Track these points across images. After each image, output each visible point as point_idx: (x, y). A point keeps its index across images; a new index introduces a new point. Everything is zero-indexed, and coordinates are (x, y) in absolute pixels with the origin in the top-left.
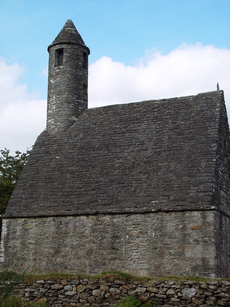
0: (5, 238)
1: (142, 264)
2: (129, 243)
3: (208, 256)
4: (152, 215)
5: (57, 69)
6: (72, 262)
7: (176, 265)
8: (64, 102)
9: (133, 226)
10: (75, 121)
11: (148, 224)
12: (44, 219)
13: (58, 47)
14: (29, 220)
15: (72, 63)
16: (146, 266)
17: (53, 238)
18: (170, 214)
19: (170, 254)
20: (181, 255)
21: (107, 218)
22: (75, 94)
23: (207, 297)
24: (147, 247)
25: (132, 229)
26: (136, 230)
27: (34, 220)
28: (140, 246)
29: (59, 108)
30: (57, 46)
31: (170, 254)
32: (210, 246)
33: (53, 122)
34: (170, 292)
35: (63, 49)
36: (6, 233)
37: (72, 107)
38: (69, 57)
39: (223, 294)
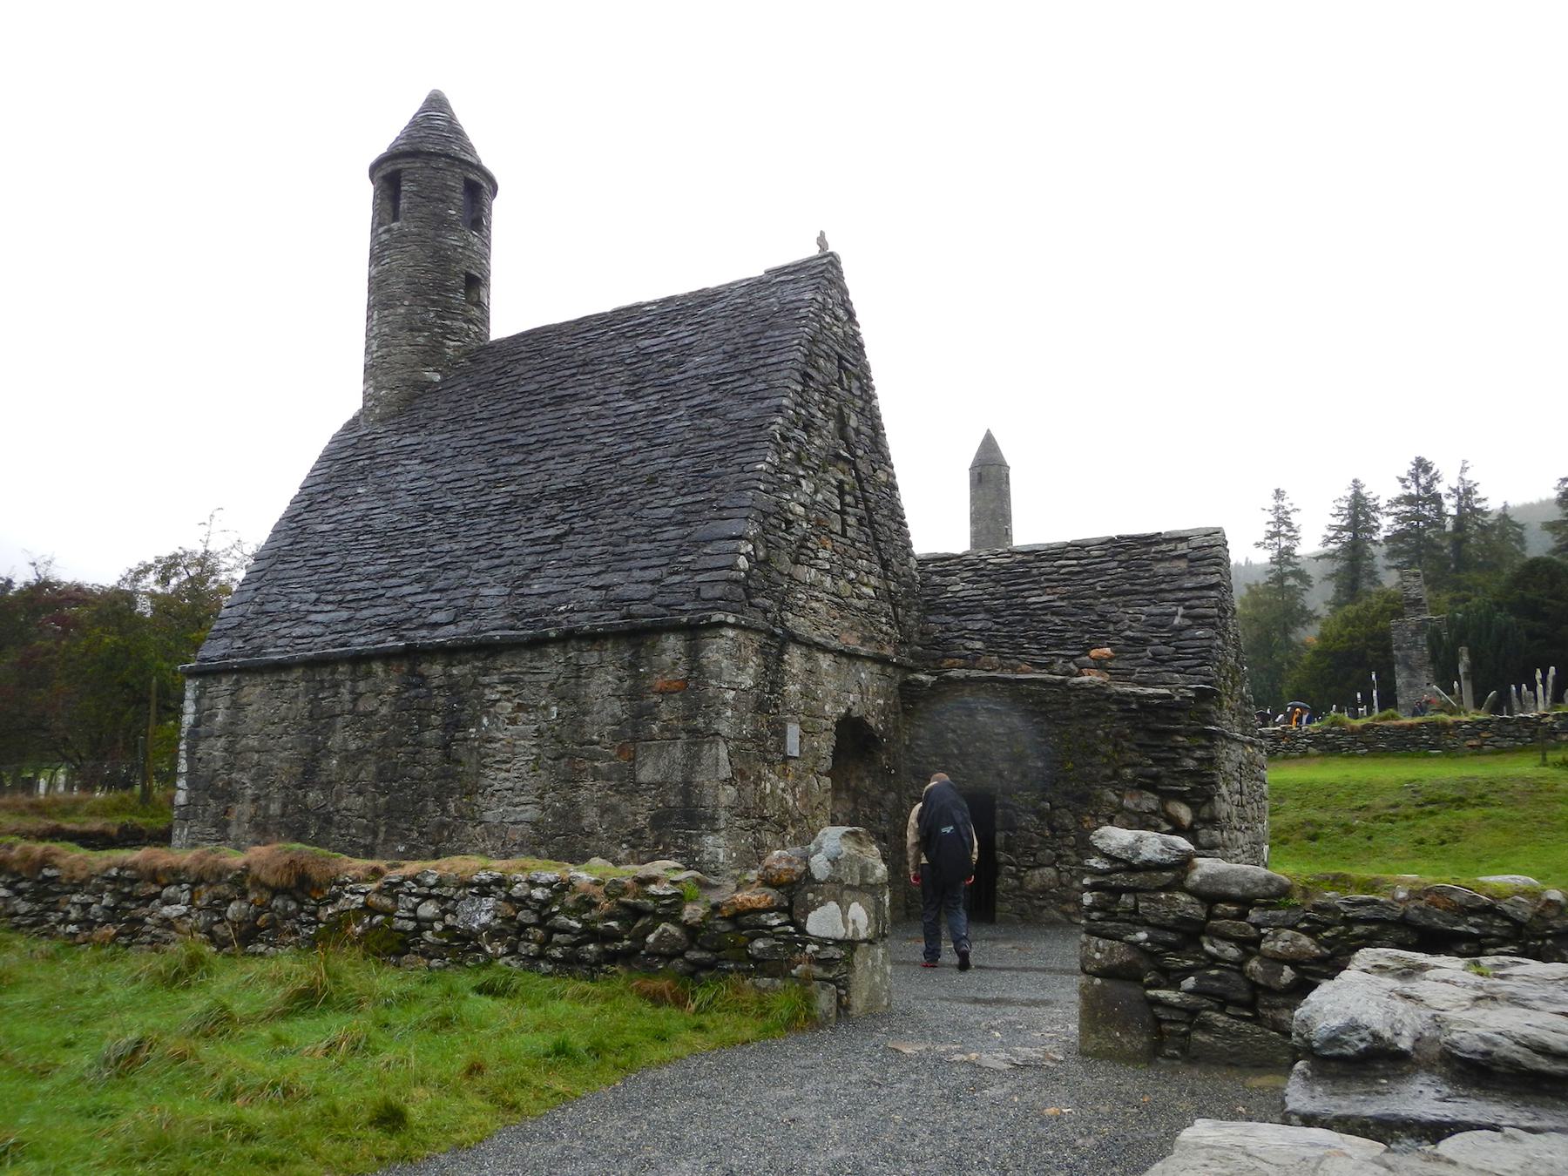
1: (522, 808)
2: (491, 742)
3: (699, 779)
4: (552, 650)
5: (384, 232)
6: (343, 804)
7: (613, 809)
8: (401, 329)
9: (500, 688)
10: (432, 382)
11: (541, 677)
12: (284, 677)
13: (388, 168)
14: (245, 682)
15: (424, 210)
16: (531, 813)
17: (301, 732)
18: (601, 646)
19: (596, 773)
21: (435, 670)
22: (434, 302)
23: (523, 927)
24: (535, 750)
25: (498, 696)
26: (509, 700)
28: (517, 750)
29: (387, 346)
30: (384, 166)
31: (596, 773)
32: (707, 746)
35: (400, 171)
37: (421, 340)
38: (416, 194)
39: (562, 919)
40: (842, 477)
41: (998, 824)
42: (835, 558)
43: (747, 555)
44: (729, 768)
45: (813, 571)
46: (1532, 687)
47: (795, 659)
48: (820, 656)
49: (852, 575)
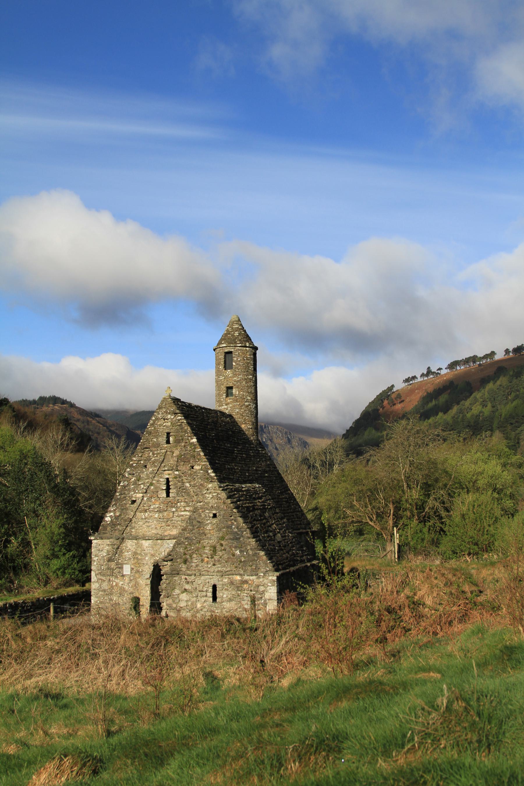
40: (167, 476)
42: (161, 507)
43: (111, 517)
44: (96, 578)
45: (147, 514)
47: (130, 544)
48: (144, 542)
49: (174, 509)
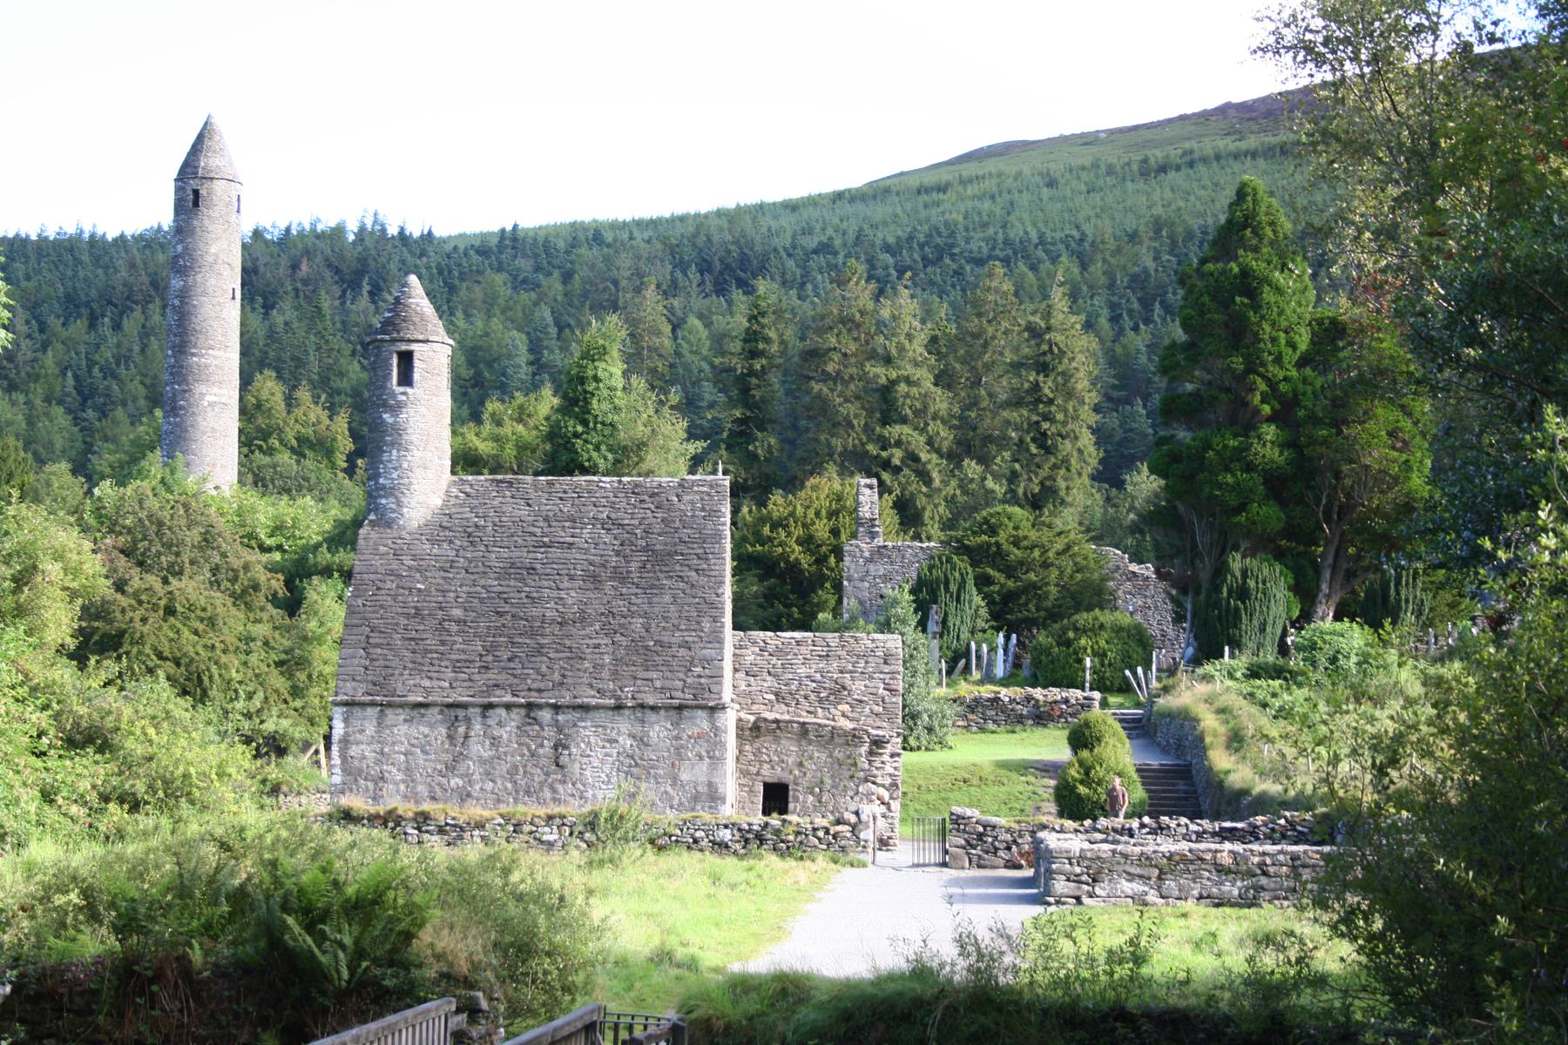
0: (340, 741)
4: (627, 712)
12: (422, 711)
14: (389, 711)
20: (675, 780)
27: (401, 711)
33: (393, 506)
34: (699, 834)
36: (342, 732)
41: (791, 799)
46: (992, 650)
